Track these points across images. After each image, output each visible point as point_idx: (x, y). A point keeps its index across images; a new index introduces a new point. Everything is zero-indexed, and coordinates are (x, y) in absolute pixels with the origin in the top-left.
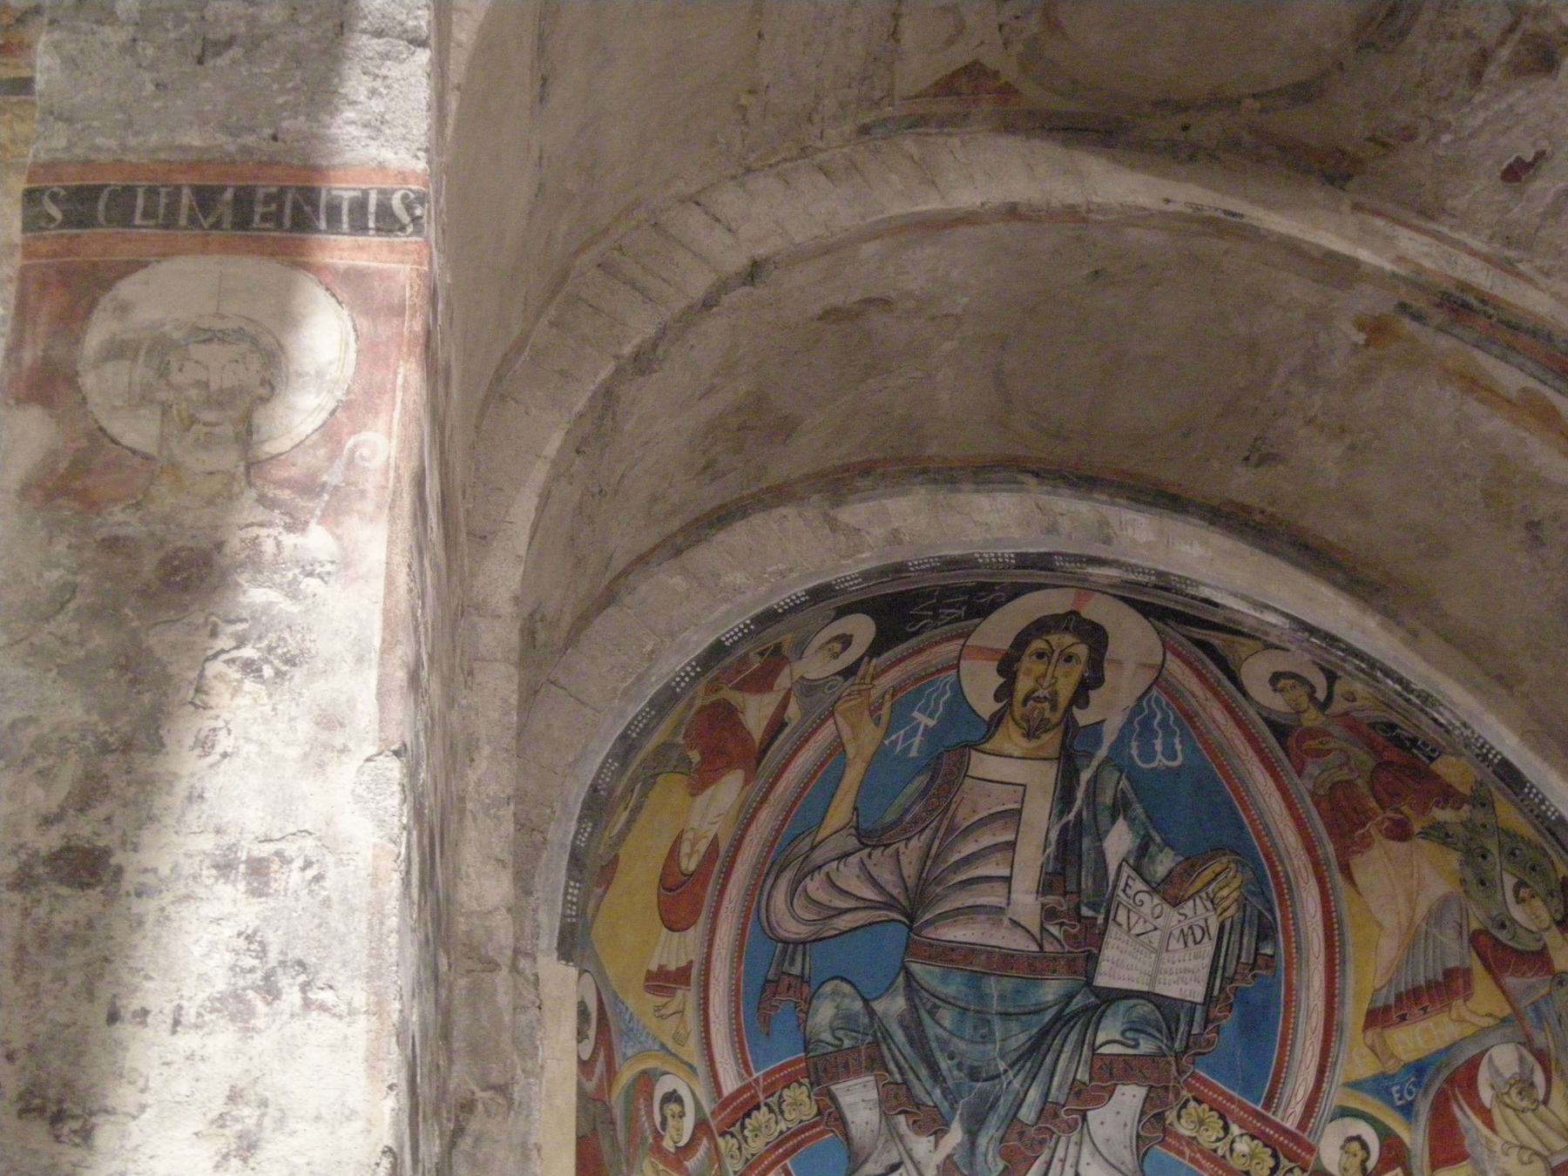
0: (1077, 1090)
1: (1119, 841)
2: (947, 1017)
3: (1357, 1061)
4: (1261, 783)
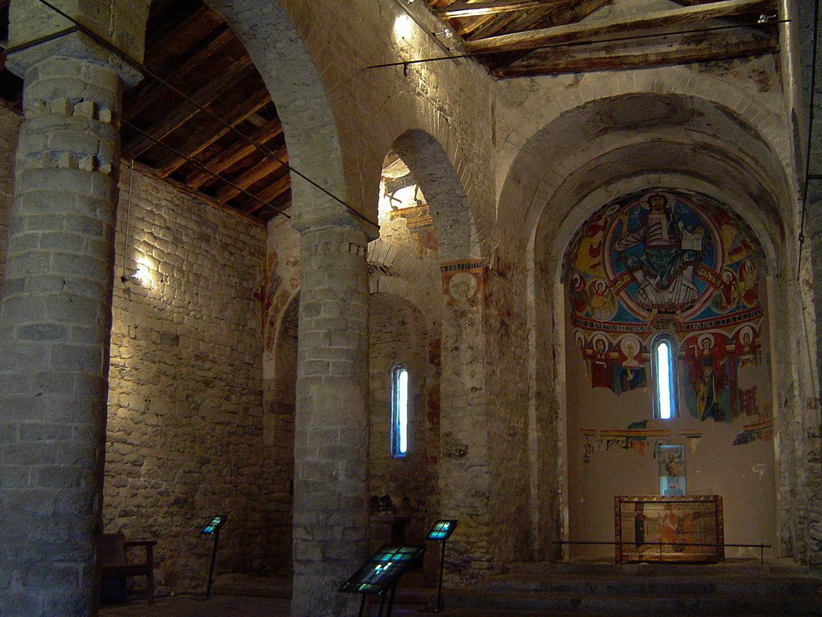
0: (681, 268)
1: (681, 225)
2: (654, 258)
3: (727, 262)
4: (703, 215)
